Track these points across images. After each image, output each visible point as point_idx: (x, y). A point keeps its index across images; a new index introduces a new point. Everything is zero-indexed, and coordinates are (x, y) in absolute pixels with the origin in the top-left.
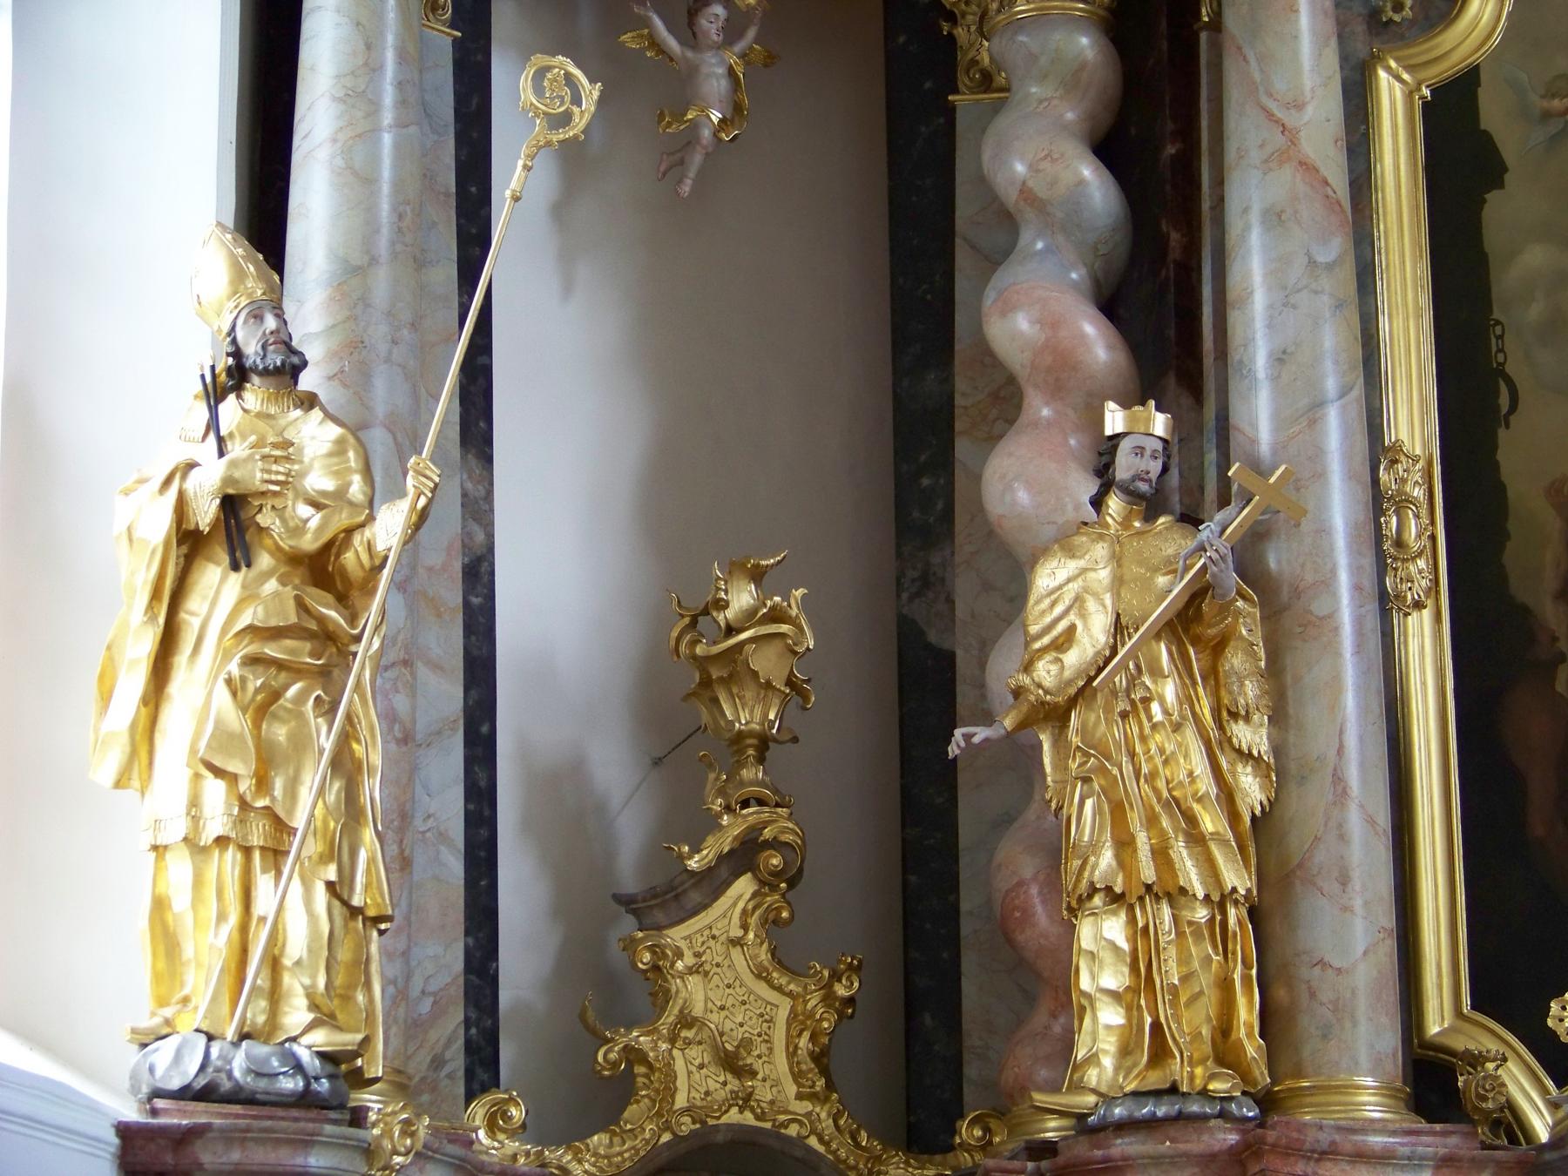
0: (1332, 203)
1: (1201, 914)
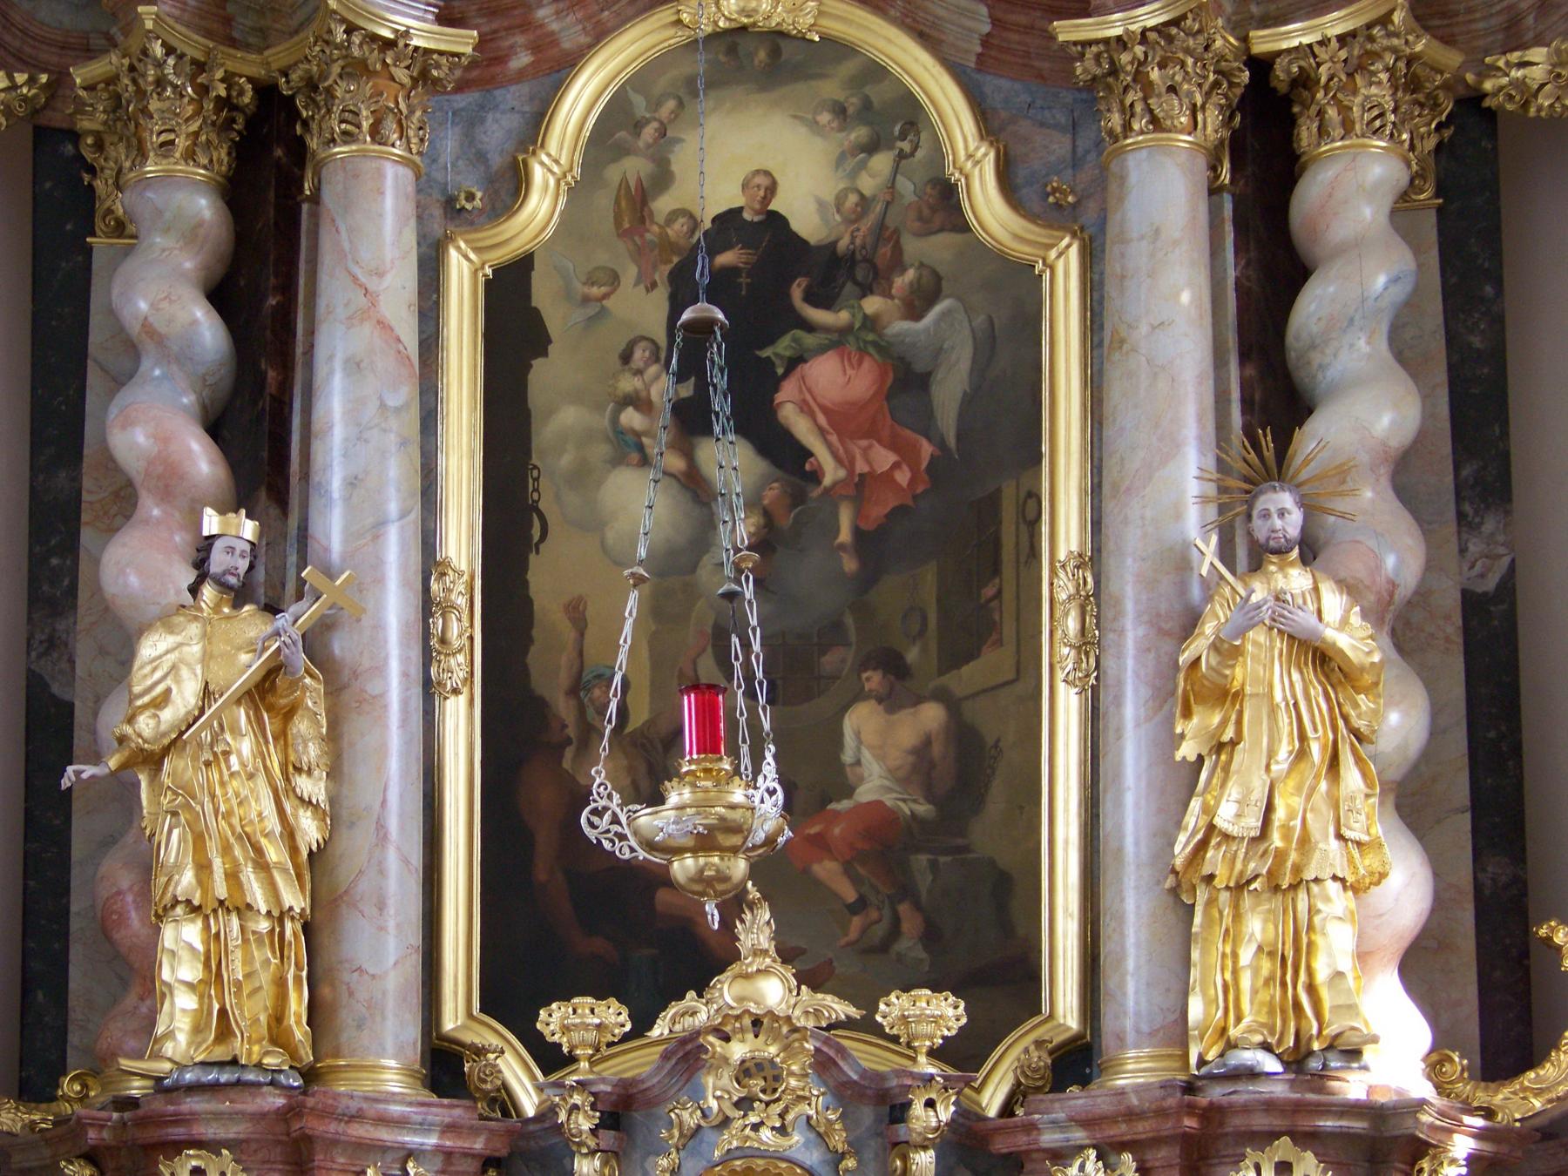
0: (402, 357)
1: (264, 926)
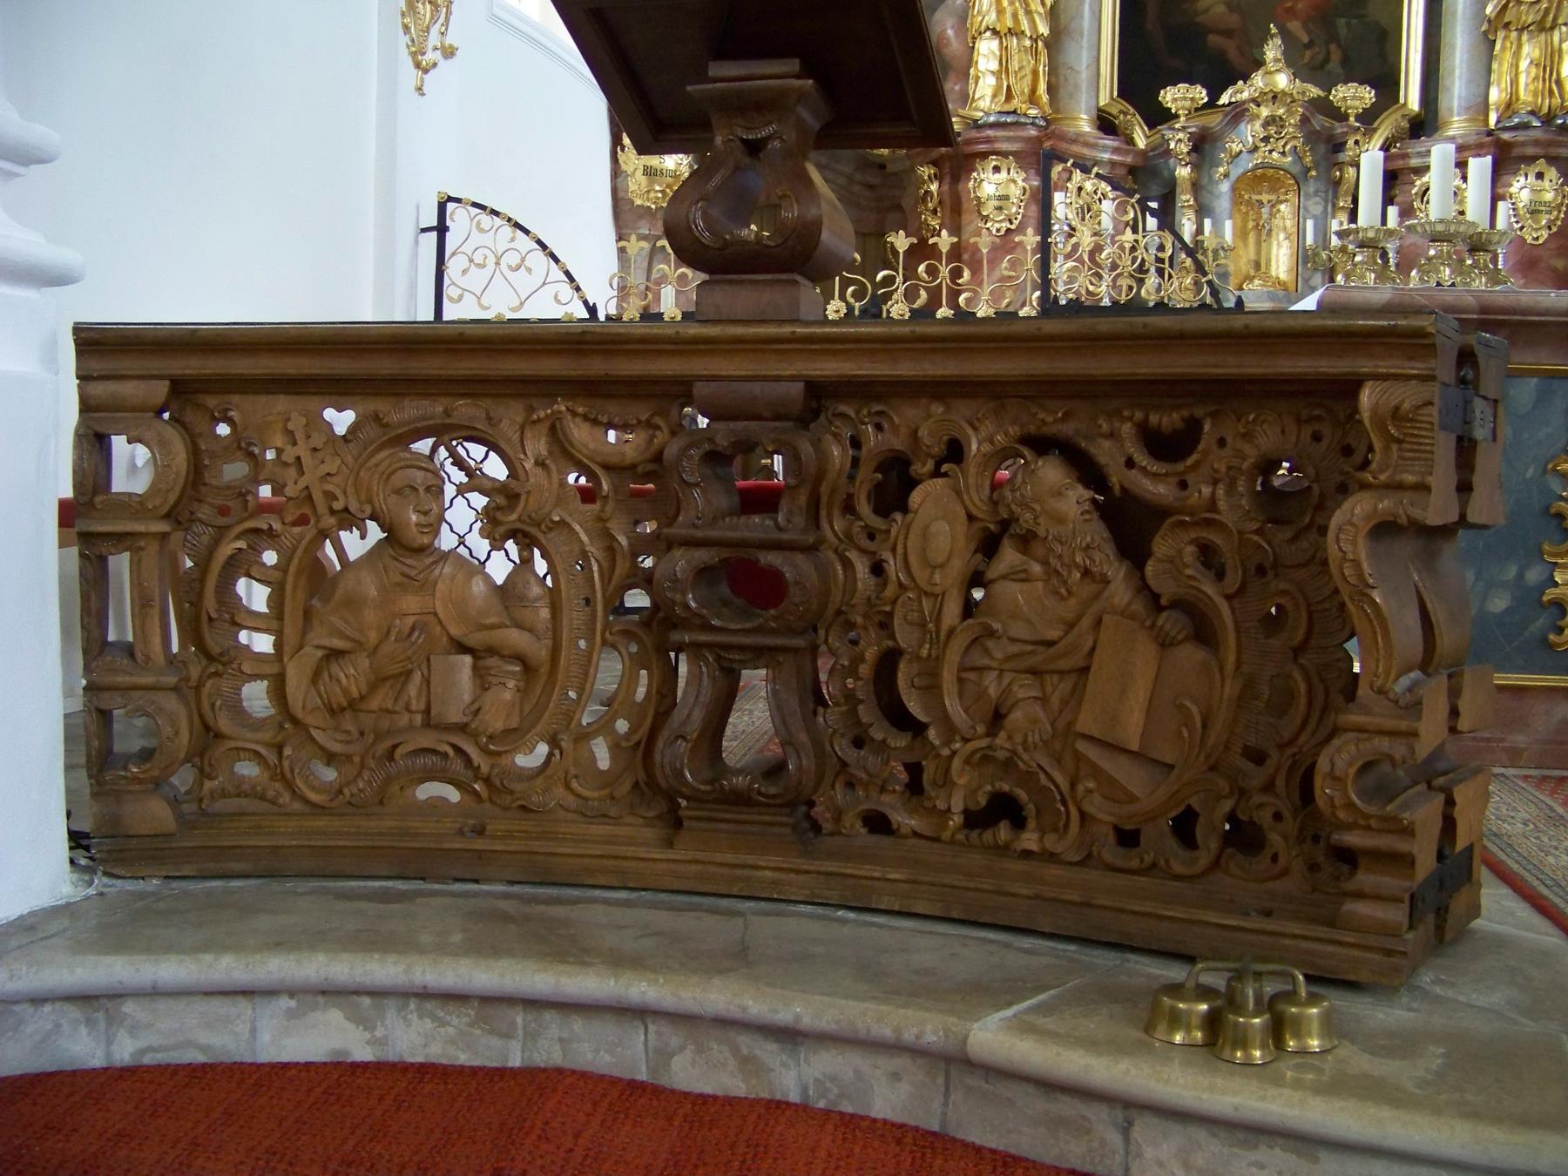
1: (1028, 43)
